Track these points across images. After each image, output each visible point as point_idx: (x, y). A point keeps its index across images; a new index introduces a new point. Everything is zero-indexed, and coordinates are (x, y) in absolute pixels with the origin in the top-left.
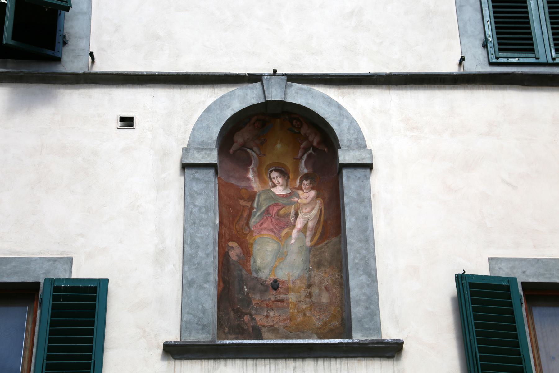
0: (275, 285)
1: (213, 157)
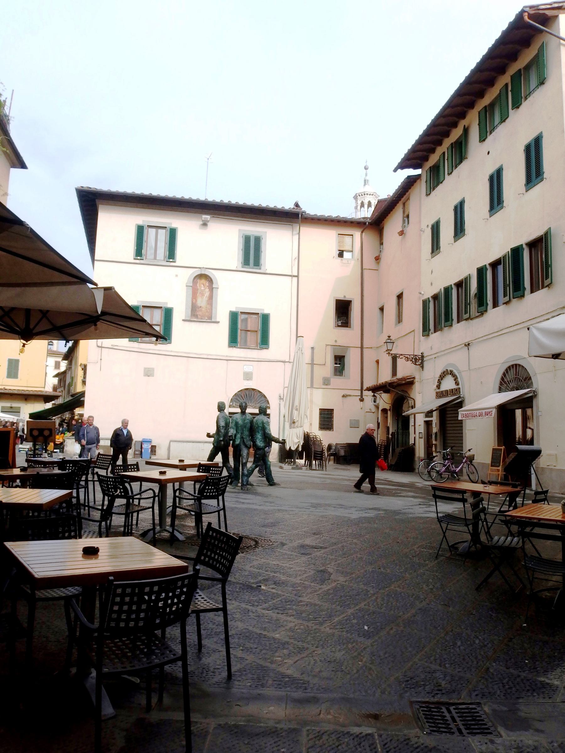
0: (201, 307)
1: (191, 285)
